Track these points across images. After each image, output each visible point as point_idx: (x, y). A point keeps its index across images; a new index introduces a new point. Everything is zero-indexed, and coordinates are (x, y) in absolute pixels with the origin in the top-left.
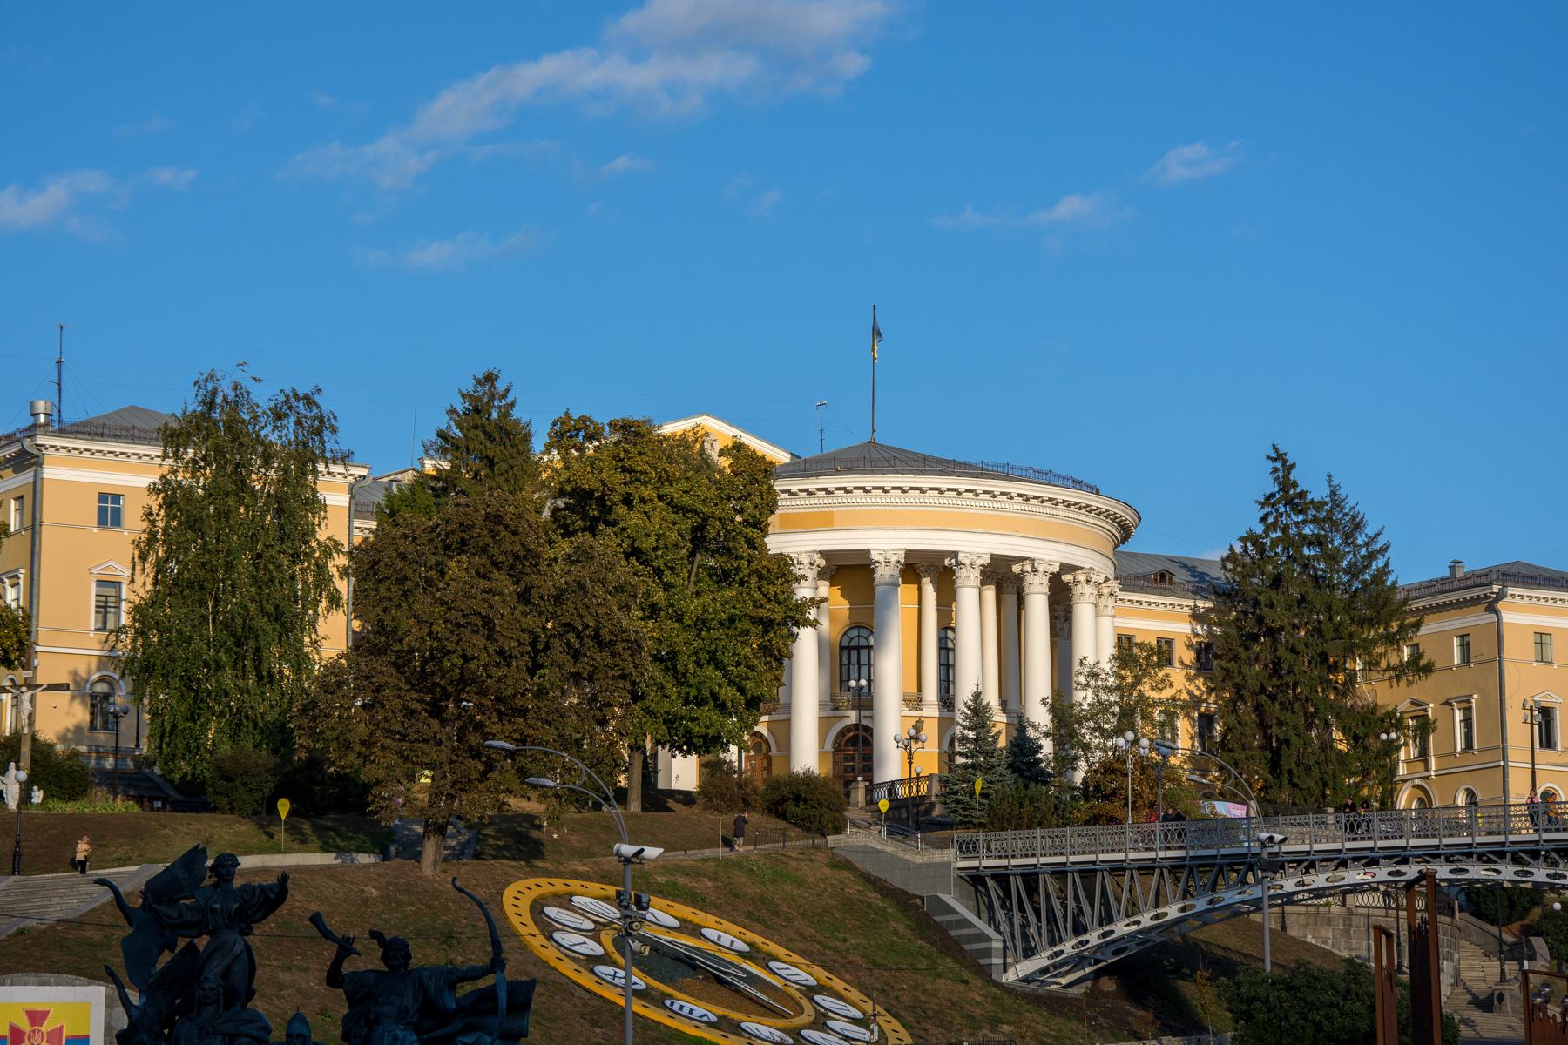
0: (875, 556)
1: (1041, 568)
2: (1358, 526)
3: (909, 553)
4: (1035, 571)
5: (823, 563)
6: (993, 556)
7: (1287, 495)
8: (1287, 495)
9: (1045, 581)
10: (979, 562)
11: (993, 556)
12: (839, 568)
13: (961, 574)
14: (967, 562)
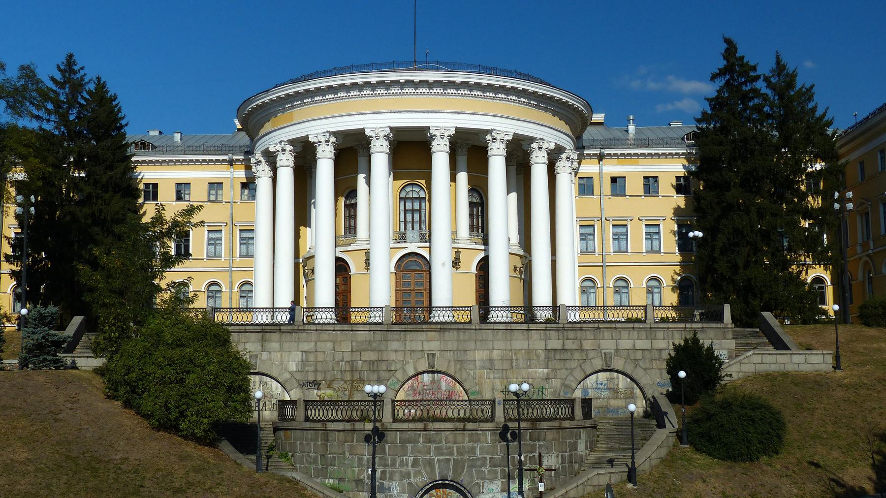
1: (438, 134)
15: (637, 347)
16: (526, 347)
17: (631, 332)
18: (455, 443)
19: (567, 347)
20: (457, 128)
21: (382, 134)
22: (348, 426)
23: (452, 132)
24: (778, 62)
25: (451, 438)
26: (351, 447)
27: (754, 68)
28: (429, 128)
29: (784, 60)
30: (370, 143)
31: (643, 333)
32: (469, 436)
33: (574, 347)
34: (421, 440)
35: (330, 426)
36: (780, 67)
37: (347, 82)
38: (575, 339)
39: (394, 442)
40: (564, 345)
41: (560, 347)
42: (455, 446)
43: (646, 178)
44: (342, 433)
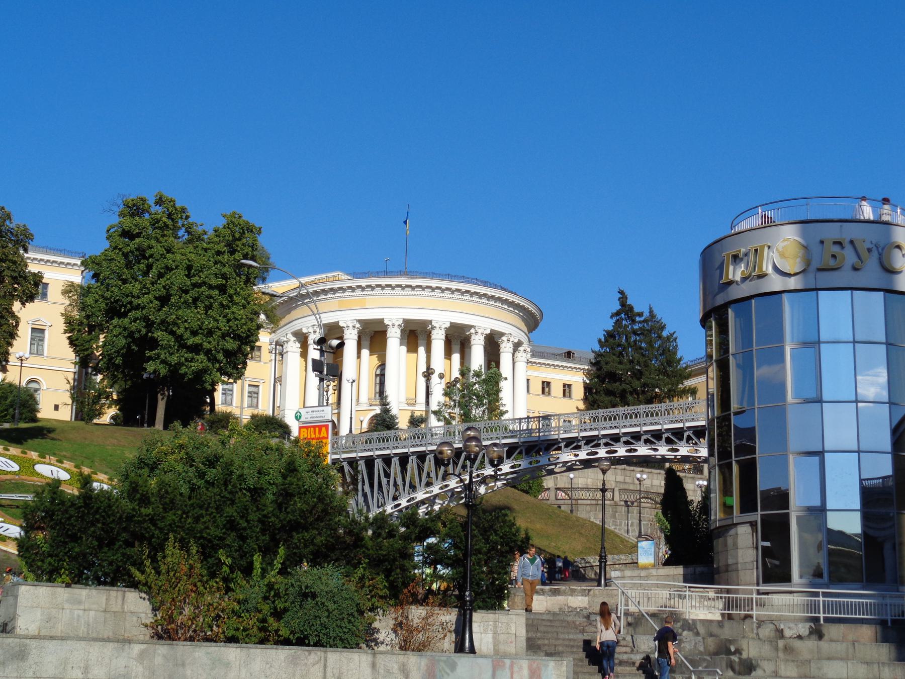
0: (386, 322)
1: (480, 331)
2: (663, 328)
3: (406, 322)
4: (476, 333)
5: (358, 325)
7: (626, 310)
8: (626, 310)
9: (482, 338)
12: (376, 332)
13: (434, 332)
20: (492, 330)
21: (397, 324)
22: (594, 502)
23: (488, 332)
24: (651, 311)
27: (640, 314)
28: (471, 327)
29: (656, 311)
35: (580, 502)
37: (424, 285)
39: (621, 512)
43: (543, 382)
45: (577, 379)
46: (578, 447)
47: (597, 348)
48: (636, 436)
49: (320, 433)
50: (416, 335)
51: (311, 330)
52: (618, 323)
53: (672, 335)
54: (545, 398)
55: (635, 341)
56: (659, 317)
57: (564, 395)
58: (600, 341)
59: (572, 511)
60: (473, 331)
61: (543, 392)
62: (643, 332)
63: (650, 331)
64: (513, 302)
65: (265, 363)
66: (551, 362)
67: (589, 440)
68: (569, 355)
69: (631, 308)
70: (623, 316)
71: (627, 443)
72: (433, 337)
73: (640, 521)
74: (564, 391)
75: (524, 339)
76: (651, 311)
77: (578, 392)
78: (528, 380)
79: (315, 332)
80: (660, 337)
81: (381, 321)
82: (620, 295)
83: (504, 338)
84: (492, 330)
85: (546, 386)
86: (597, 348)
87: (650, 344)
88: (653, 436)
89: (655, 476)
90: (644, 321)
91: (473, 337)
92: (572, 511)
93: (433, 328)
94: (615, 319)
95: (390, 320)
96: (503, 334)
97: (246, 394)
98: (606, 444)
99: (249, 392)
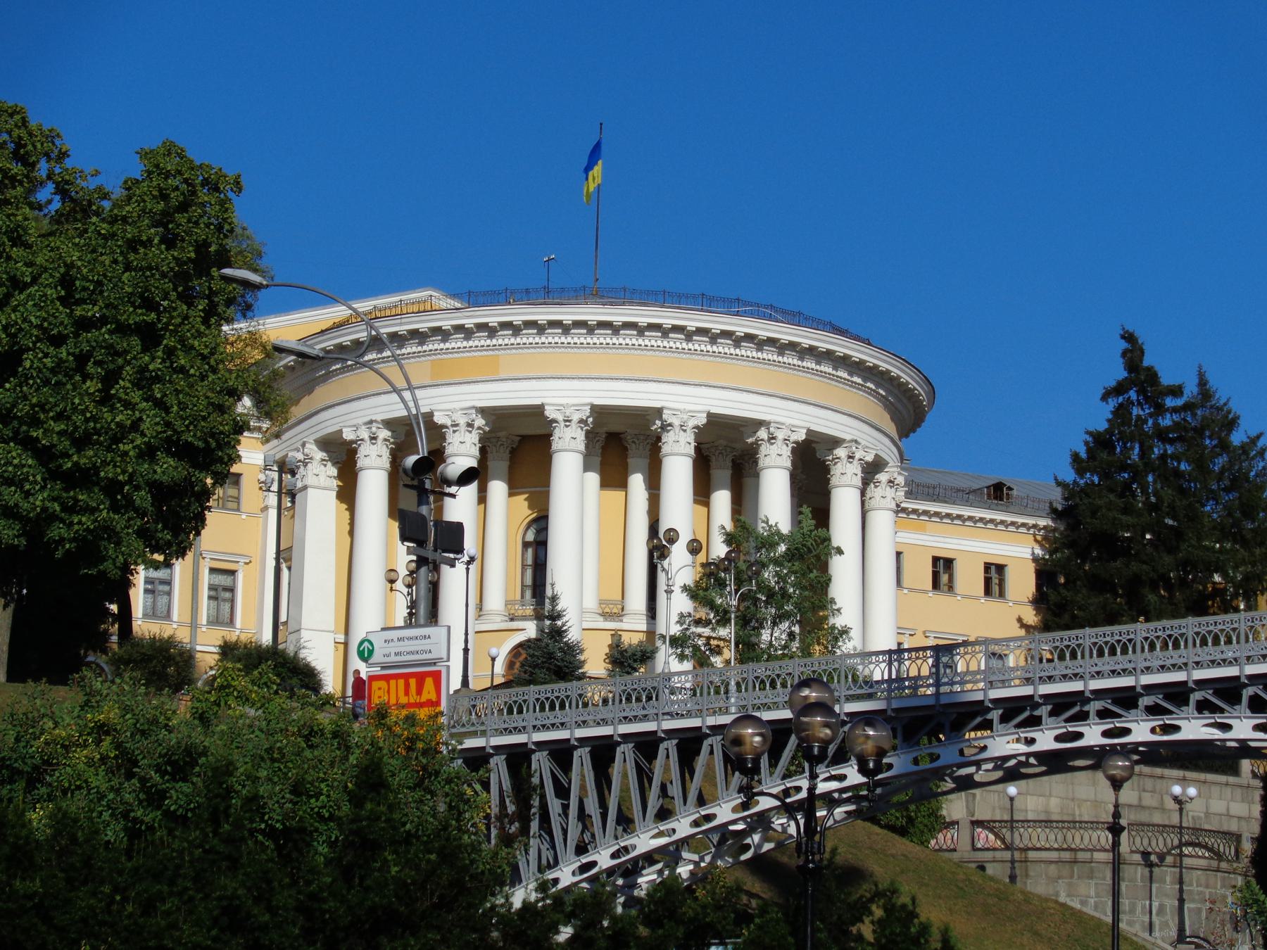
0: (550, 413)
1: (780, 435)
2: (1231, 424)
3: (600, 412)
4: (772, 438)
5: (480, 422)
6: (710, 415)
8: (1139, 379)
9: (787, 451)
10: (692, 423)
11: (710, 415)
12: (524, 439)
14: (676, 422)
15: (1232, 812)
16: (1092, 797)
17: (1224, 788)
18: (1207, 886)
19: (1145, 803)
20: (810, 432)
21: (576, 417)
22: (1066, 855)
23: (801, 436)
24: (1202, 383)
25: (1203, 880)
26: (1070, 885)
27: (1176, 391)
28: (760, 424)
29: (1213, 382)
30: (659, 439)
31: (1239, 791)
32: (1223, 879)
33: (1154, 803)
34: (1168, 879)
35: (1031, 854)
36: (1205, 392)
38: (1153, 791)
39: (1133, 880)
40: (1140, 799)
41: (1135, 802)
42: (1207, 891)
43: (936, 560)
44: (1053, 867)
45: (1019, 552)
46: (1034, 722)
47: (1069, 475)
48: (1177, 695)
49: (419, 692)
50: (622, 444)
51: (364, 434)
52: (1121, 413)
53: (1254, 441)
54: (941, 600)
55: (1163, 457)
56: (1221, 396)
57: (988, 592)
58: (1075, 457)
59: (1013, 878)
60: (763, 434)
61: (936, 585)
62: (1185, 435)
63: (1199, 431)
64: (862, 362)
65: (250, 515)
66: (955, 511)
67: (1060, 704)
68: (998, 493)
69: (1152, 376)
70: (1133, 394)
71: (1154, 710)
72: (665, 449)
73: (1181, 901)
74: (988, 582)
75: (889, 453)
76: (1202, 383)
77: (1022, 583)
78: (899, 554)
79: (373, 438)
80: (1224, 446)
81: (537, 412)
82: (1124, 345)
83: (841, 452)
84: (810, 432)
85: (943, 568)
86: (1069, 475)
87: (1201, 465)
88: (1217, 693)
89: (1215, 790)
90: (1188, 407)
91: (764, 449)
92: (1013, 878)
93: (666, 427)
94: (1113, 403)
95: (560, 407)
96: (836, 442)
97: (204, 593)
98: (1104, 714)
99: (211, 588)
